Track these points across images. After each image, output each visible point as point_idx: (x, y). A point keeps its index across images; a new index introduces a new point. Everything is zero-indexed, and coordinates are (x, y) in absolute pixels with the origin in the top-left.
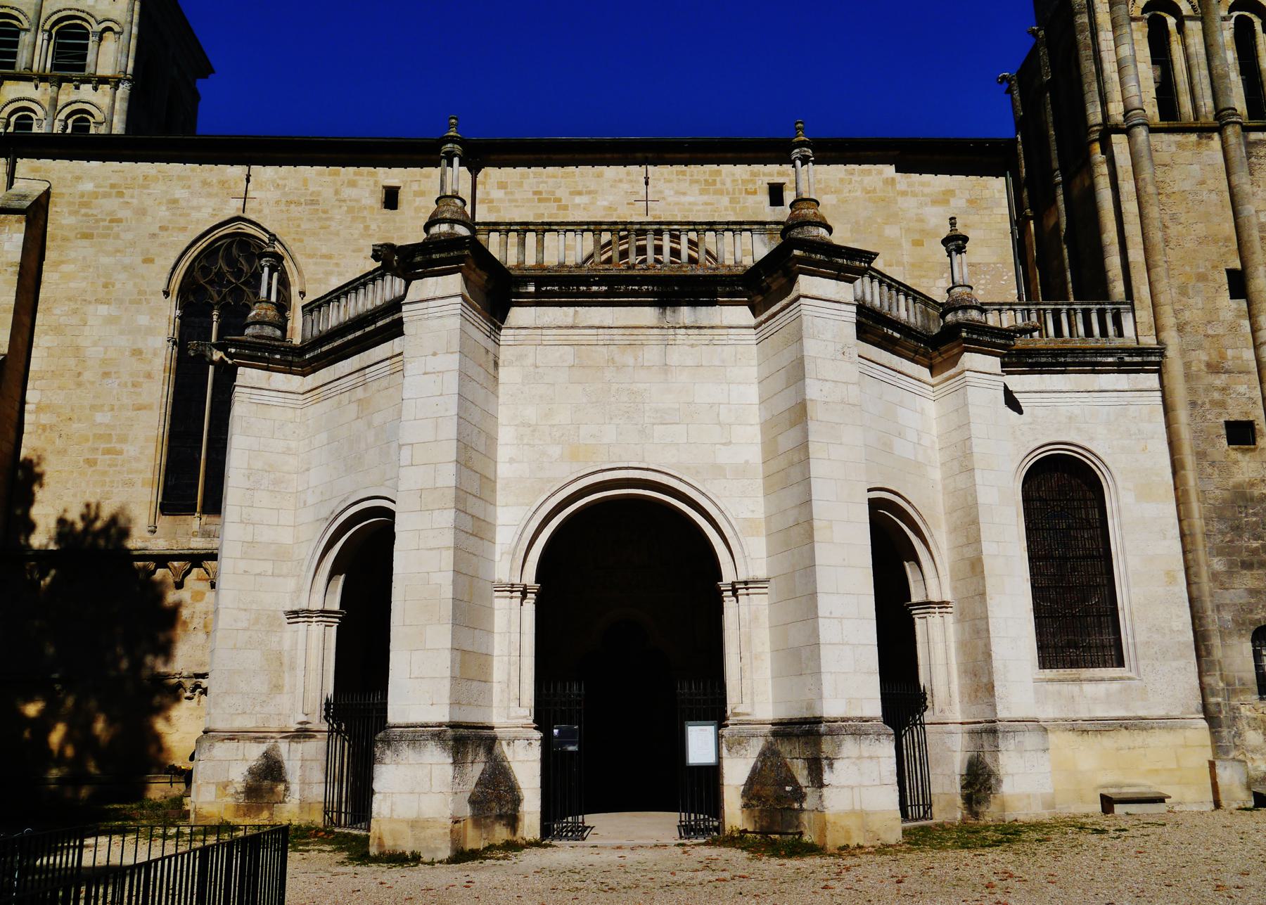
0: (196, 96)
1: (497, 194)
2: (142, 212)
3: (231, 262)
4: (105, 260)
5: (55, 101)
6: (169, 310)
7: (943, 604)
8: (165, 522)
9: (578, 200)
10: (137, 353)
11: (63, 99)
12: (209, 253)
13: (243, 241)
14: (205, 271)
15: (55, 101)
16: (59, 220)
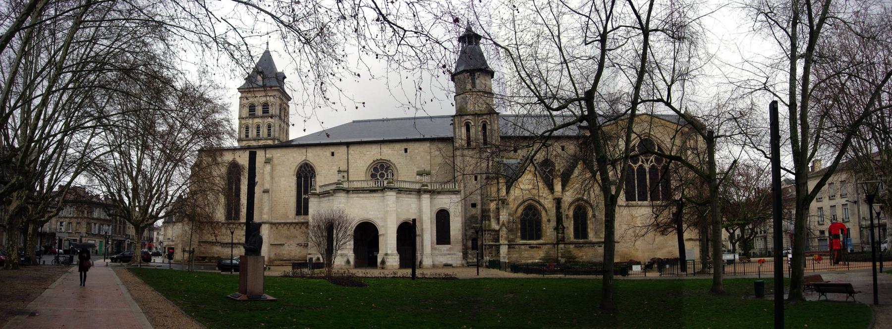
0: (288, 106)
1: (352, 152)
2: (288, 159)
3: (304, 168)
4: (283, 169)
5: (264, 122)
6: (295, 178)
7: (419, 235)
8: (297, 217)
9: (368, 153)
10: (290, 186)
11: (266, 121)
12: (301, 167)
13: (306, 164)
14: (300, 170)
15: (264, 122)
16: (275, 161)
